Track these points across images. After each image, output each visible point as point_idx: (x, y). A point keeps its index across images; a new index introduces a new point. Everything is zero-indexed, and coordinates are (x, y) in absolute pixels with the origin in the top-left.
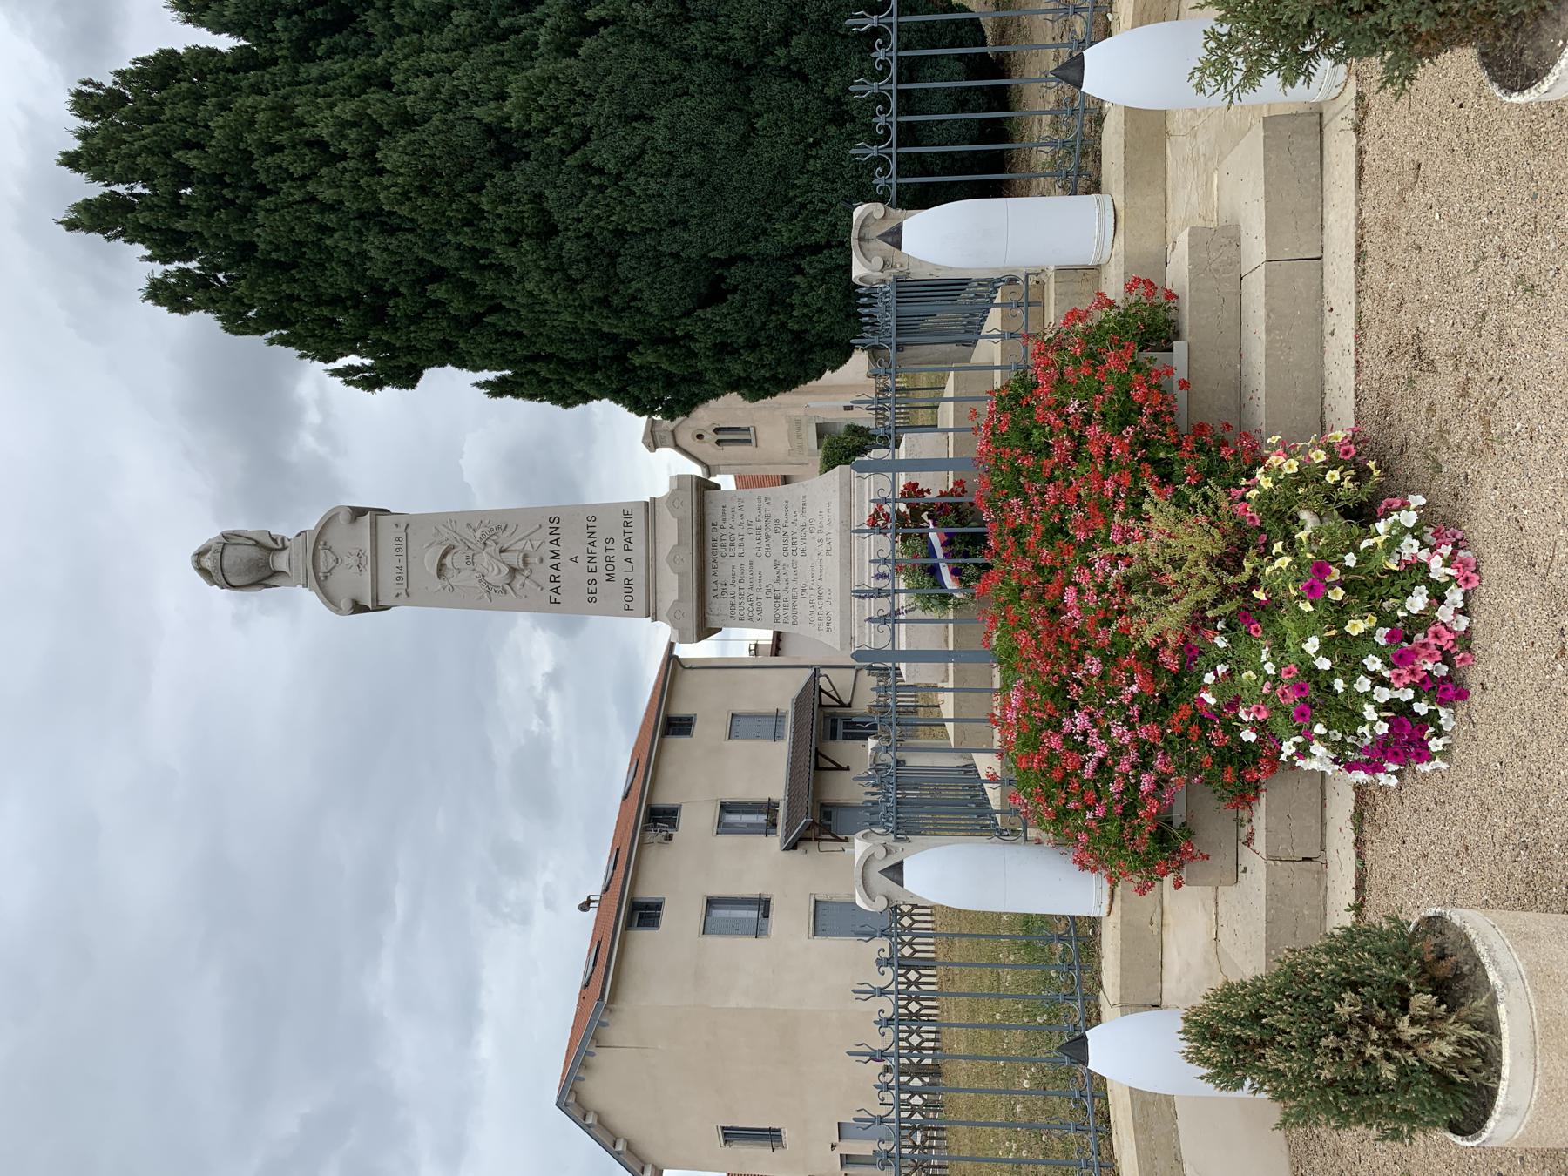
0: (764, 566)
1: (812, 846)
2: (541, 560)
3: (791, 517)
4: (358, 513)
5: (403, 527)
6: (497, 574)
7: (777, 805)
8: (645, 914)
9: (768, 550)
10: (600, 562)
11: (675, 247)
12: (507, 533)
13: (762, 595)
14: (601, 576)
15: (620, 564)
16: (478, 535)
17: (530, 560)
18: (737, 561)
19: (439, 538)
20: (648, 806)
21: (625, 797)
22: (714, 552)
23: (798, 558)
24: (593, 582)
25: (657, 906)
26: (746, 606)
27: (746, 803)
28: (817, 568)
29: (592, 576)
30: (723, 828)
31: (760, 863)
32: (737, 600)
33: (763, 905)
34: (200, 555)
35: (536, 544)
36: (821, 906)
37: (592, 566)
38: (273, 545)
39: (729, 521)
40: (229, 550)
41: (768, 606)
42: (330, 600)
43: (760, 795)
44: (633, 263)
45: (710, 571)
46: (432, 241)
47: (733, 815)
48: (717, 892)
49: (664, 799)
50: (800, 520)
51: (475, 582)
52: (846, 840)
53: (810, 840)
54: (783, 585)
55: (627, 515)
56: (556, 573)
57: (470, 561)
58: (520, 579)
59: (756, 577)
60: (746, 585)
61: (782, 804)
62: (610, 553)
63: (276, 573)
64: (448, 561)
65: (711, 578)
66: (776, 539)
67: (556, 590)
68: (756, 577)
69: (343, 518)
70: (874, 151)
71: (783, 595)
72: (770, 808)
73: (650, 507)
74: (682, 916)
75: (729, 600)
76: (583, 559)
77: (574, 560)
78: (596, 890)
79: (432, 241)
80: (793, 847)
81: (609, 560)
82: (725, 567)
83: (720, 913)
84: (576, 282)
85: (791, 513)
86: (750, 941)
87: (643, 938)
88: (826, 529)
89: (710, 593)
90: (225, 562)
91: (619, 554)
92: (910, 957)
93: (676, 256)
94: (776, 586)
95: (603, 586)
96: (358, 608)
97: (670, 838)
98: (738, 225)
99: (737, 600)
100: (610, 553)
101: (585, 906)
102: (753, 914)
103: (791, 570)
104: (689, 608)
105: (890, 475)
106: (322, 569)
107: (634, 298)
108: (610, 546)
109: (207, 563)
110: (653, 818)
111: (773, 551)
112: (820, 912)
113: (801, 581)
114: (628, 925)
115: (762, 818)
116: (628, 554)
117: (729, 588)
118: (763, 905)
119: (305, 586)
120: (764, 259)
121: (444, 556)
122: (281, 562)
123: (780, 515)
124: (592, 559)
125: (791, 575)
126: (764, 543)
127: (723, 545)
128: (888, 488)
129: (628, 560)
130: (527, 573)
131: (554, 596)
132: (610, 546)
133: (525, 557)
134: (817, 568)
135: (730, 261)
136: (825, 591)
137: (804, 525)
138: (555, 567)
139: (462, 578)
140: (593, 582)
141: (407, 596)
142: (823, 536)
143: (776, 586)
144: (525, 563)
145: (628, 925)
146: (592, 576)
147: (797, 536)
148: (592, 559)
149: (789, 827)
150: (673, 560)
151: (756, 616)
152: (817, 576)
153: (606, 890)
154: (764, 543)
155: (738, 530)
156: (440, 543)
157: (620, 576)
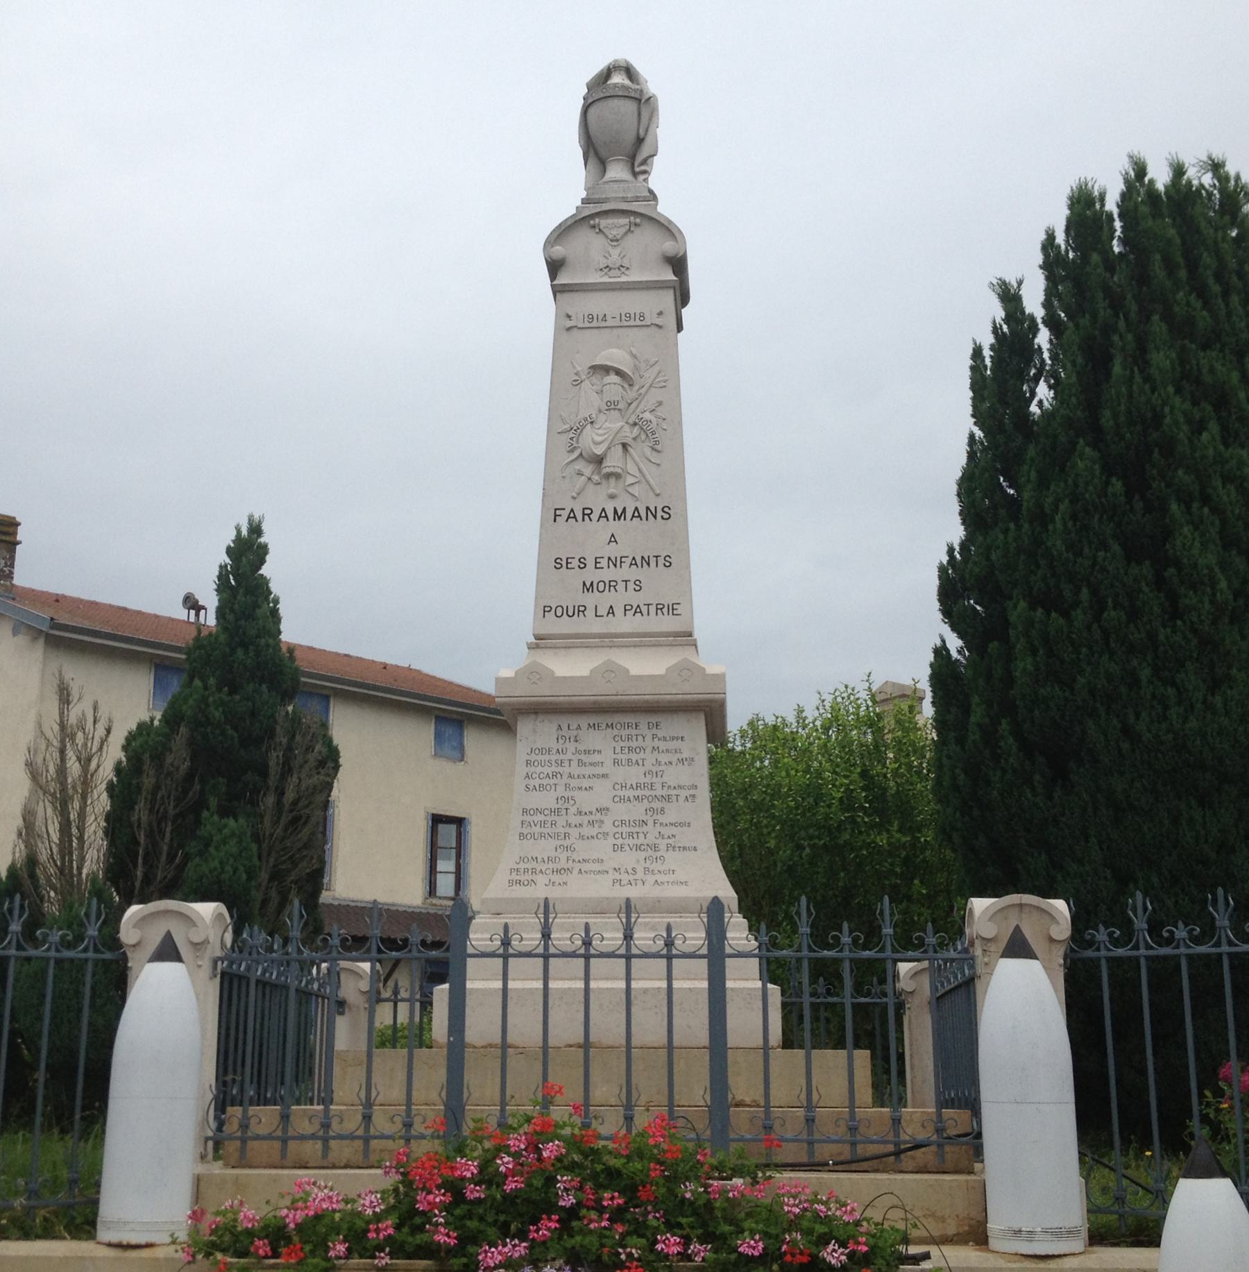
0: (601, 794)
2: (612, 497)
3: (667, 831)
4: (678, 264)
5: (658, 321)
6: (594, 440)
9: (622, 799)
10: (608, 574)
12: (648, 451)
13: (561, 791)
14: (591, 575)
15: (604, 600)
16: (647, 416)
18: (607, 756)
19: (643, 366)
22: (623, 726)
23: (611, 841)
24: (583, 565)
26: (547, 770)
28: (596, 867)
29: (590, 563)
32: (553, 758)
34: (629, 71)
35: (635, 490)
37: (604, 563)
38: (639, 159)
39: (663, 745)
40: (630, 106)
41: (546, 800)
42: (563, 232)
45: (594, 719)
50: (662, 844)
51: (584, 413)
54: (574, 820)
55: (672, 609)
56: (595, 516)
57: (611, 406)
58: (588, 470)
59: (585, 783)
60: (575, 770)
62: (621, 586)
63: (603, 164)
64: (613, 378)
65: (584, 721)
66: (637, 811)
67: (572, 516)
68: (585, 783)
69: (669, 247)
70: (1140, 923)
71: (561, 821)
73: (685, 637)
75: (554, 746)
76: (613, 551)
77: (613, 539)
81: (611, 585)
82: (599, 741)
85: (673, 830)
88: (650, 879)
89: (564, 721)
90: (616, 102)
91: (618, 599)
94: (573, 810)
95: (575, 578)
96: (554, 267)
100: (621, 586)
103: (594, 831)
104: (542, 691)
105: (704, 951)
106: (604, 222)
108: (631, 586)
109: (618, 79)
111: (621, 806)
116: (619, 611)
117: (571, 747)
119: (585, 201)
121: (618, 372)
122: (617, 171)
123: (672, 814)
124: (614, 562)
125: (587, 831)
126: (631, 793)
127: (629, 738)
129: (611, 611)
130: (596, 478)
131: (565, 514)
132: (631, 586)
133: (617, 476)
134: (596, 867)
136: (564, 878)
137: (655, 848)
138: (603, 515)
139: (589, 399)
140: (583, 565)
141: (567, 327)
142: (640, 875)
143: (573, 810)
144: (608, 476)
146: (590, 563)
147: (641, 840)
148: (614, 562)
150: (610, 669)
151: (532, 783)
152: (585, 867)
154: (631, 793)
155: (650, 758)
156: (636, 368)
157: (590, 600)
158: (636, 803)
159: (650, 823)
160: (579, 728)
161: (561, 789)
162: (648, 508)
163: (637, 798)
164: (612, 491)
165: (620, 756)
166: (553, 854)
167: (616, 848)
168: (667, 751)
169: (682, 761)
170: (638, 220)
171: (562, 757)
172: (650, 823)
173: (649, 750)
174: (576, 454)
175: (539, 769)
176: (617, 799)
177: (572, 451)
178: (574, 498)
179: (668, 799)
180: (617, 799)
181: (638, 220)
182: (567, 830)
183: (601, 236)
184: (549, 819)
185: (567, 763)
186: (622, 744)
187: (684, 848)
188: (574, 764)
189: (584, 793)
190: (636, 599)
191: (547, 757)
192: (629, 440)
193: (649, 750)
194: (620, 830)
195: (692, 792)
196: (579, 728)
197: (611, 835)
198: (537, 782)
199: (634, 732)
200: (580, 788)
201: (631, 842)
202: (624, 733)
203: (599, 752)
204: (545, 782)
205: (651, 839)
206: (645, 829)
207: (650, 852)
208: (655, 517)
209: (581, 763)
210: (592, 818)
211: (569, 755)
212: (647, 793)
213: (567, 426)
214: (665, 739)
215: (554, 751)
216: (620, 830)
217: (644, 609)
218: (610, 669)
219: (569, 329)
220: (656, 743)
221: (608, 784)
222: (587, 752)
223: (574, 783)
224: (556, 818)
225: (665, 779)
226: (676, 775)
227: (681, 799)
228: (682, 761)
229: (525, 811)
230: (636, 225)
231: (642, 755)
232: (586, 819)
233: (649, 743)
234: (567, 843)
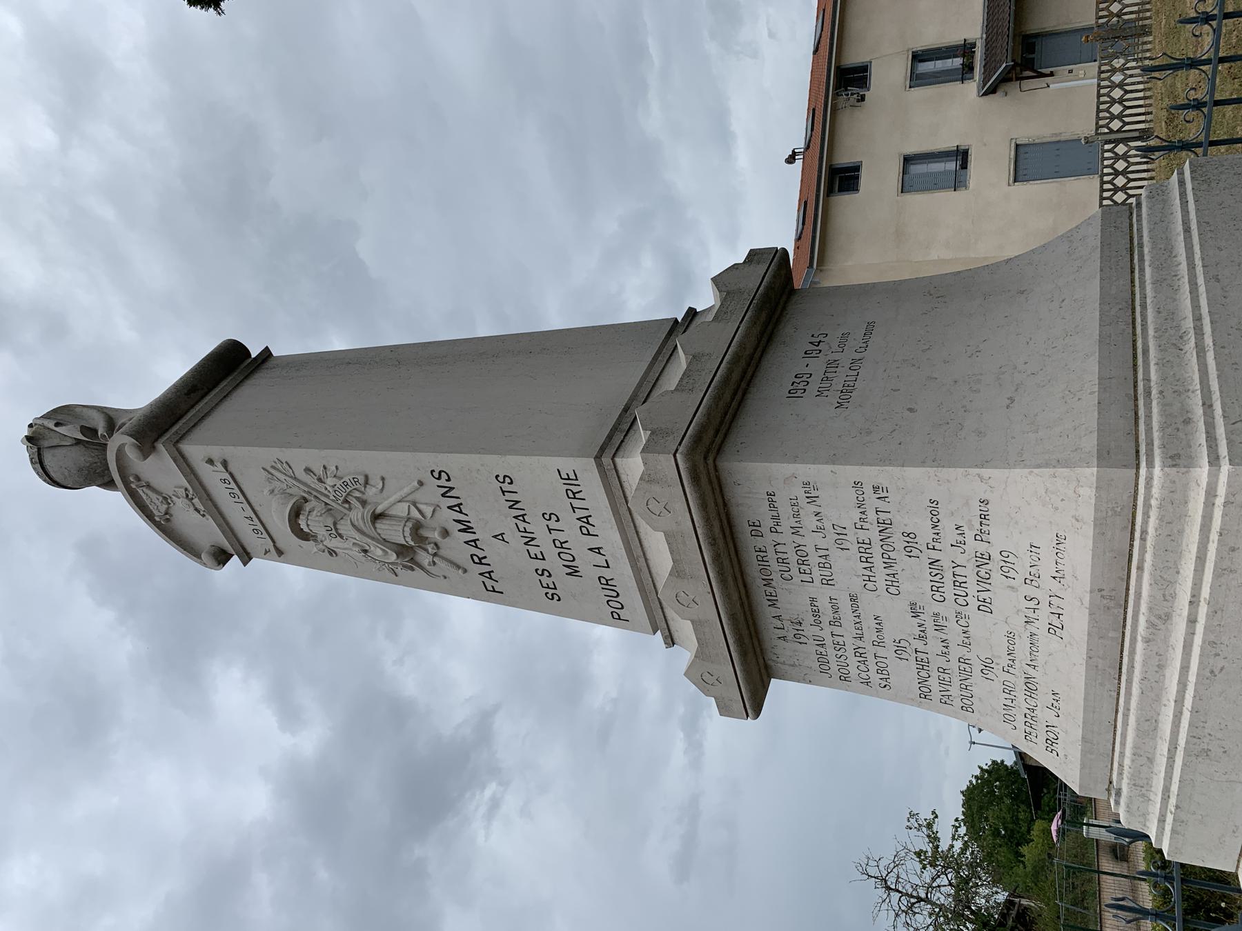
1: (1013, 87)
3: (949, 535)
7: (974, 45)
8: (843, 179)
13: (888, 652)
20: (838, 68)
21: (816, 51)
25: (856, 168)
27: (939, 49)
30: (917, 80)
31: (959, 113)
33: (962, 156)
36: (1021, 150)
39: (787, 523)
43: (955, 37)
47: (925, 66)
48: (912, 149)
49: (853, 58)
52: (1052, 74)
53: (1010, 80)
54: (934, 647)
61: (979, 44)
68: (869, 624)
72: (966, 50)
74: (880, 177)
76: (516, 540)
77: (500, 537)
78: (800, 144)
80: (992, 91)
83: (916, 169)
85: (947, 526)
86: (950, 195)
87: (844, 202)
92: (1119, 131)
94: (919, 645)
97: (863, 98)
101: (791, 159)
102: (951, 166)
110: (841, 81)
112: (1022, 156)
114: (830, 192)
115: (958, 62)
117: (809, 630)
118: (962, 156)
128: (1205, 87)
133: (417, 528)
145: (830, 192)
149: (988, 69)
151: (875, 678)
153: (808, 147)
158: (896, 567)
159: (935, 555)
161: (881, 652)
163: (888, 566)
167: (984, 606)
168: (796, 515)
176: (892, 590)
179: (884, 527)
180: (892, 590)
184: (935, 674)
186: (794, 571)
187: (984, 517)
189: (886, 626)
192: (369, 510)
194: (950, 596)
195: (868, 490)
199: (771, 555)
201: (972, 588)
202: (774, 566)
203: (813, 599)
204: (873, 668)
206: (946, 563)
207: (994, 566)
209: (835, 622)
210: (929, 624)
211: (826, 634)
212: (876, 550)
214: (776, 518)
216: (950, 596)
221: (865, 598)
222: (816, 613)
223: (871, 635)
225: (849, 524)
226: (839, 507)
227: (882, 505)
228: (812, 499)
231: (810, 549)
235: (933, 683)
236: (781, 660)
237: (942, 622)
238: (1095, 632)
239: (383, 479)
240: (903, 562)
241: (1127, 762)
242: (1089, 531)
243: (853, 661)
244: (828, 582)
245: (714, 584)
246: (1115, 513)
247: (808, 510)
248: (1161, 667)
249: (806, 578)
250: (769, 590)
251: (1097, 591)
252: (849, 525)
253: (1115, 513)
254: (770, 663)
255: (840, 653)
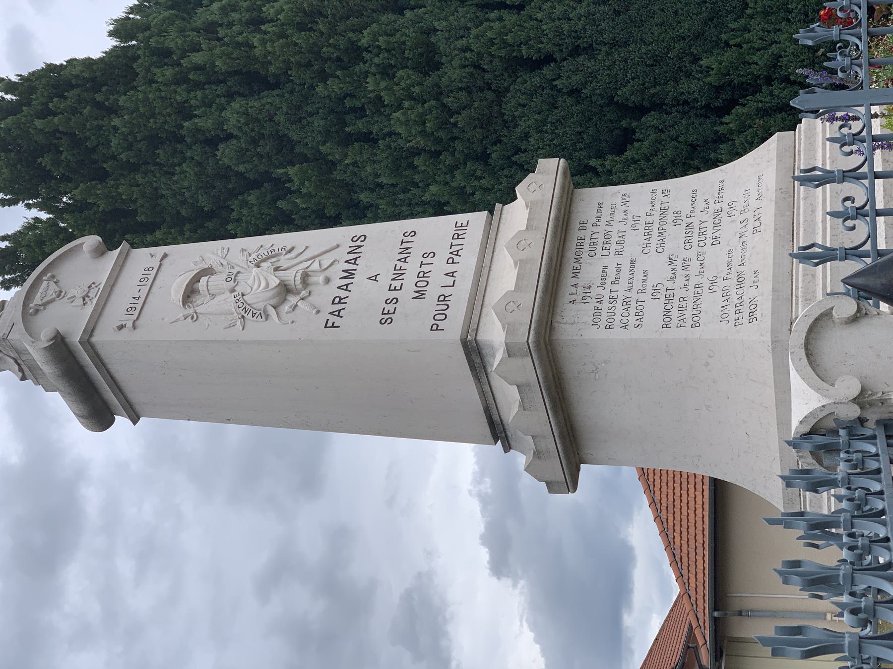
2: (328, 281)
11: (577, 79)
13: (647, 297)
17: (312, 280)
18: (611, 262)
39: (605, 217)
44: (523, 99)
45: (568, 272)
46: (299, 108)
54: (680, 281)
58: (292, 299)
59: (639, 276)
65: (568, 280)
68: (639, 276)
71: (679, 293)
75: (593, 304)
79: (299, 108)
84: (451, 113)
88: (754, 204)
91: (438, 268)
93: (575, 92)
98: (657, 61)
99: (606, 305)
106: (37, 300)
107: (518, 150)
113: (709, 274)
117: (595, 291)
120: (685, 104)
121: (196, 279)
124: (399, 274)
127: (594, 244)
135: (640, 111)
137: (718, 212)
143: (669, 285)
147: (710, 225)
157: (433, 292)
160: (575, 285)
161: (642, 297)
162: (348, 253)
163: (660, 234)
164: (321, 279)
165: (612, 251)
166: (720, 293)
167: (716, 241)
168: (612, 214)
169: (624, 203)
170: (49, 275)
171: (606, 299)
172: (690, 220)
173: (609, 228)
174: (272, 311)
175: (618, 318)
176: (660, 250)
177: (267, 317)
178: (318, 312)
181: (49, 275)
182: (691, 287)
183: (50, 306)
185: (614, 294)
188: (615, 287)
190: (444, 254)
191: (605, 312)
193: (609, 228)
196: (575, 285)
197: (700, 249)
198: (632, 320)
199: (587, 241)
200: (644, 281)
202: (587, 247)
203: (605, 267)
204: (633, 311)
205: (708, 218)
206: (696, 224)
207: (724, 215)
208: (360, 247)
209: (616, 282)
211: (606, 294)
213: (239, 323)
214: (599, 218)
215: (599, 305)
217: (454, 248)
218: (518, 243)
219: (134, 327)
220: (603, 223)
222: (604, 278)
223: (637, 285)
224: (676, 298)
227: (665, 200)
229: (666, 326)
230: (53, 277)
232: (680, 273)
233: (602, 228)
234: (706, 285)
235: (675, 313)
236: (565, 320)
237: (687, 263)
238: (779, 214)
239: (307, 247)
240: (669, 228)
241: (800, 285)
242: (775, 162)
243: (619, 308)
244: (619, 253)
245: (549, 232)
246: (786, 151)
247: (620, 209)
248: (813, 211)
249: (606, 252)
250: (577, 265)
251: (779, 190)
252: (643, 214)
253: (786, 151)
254: (556, 325)
255: (611, 306)
